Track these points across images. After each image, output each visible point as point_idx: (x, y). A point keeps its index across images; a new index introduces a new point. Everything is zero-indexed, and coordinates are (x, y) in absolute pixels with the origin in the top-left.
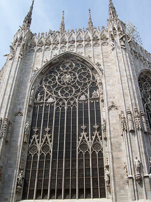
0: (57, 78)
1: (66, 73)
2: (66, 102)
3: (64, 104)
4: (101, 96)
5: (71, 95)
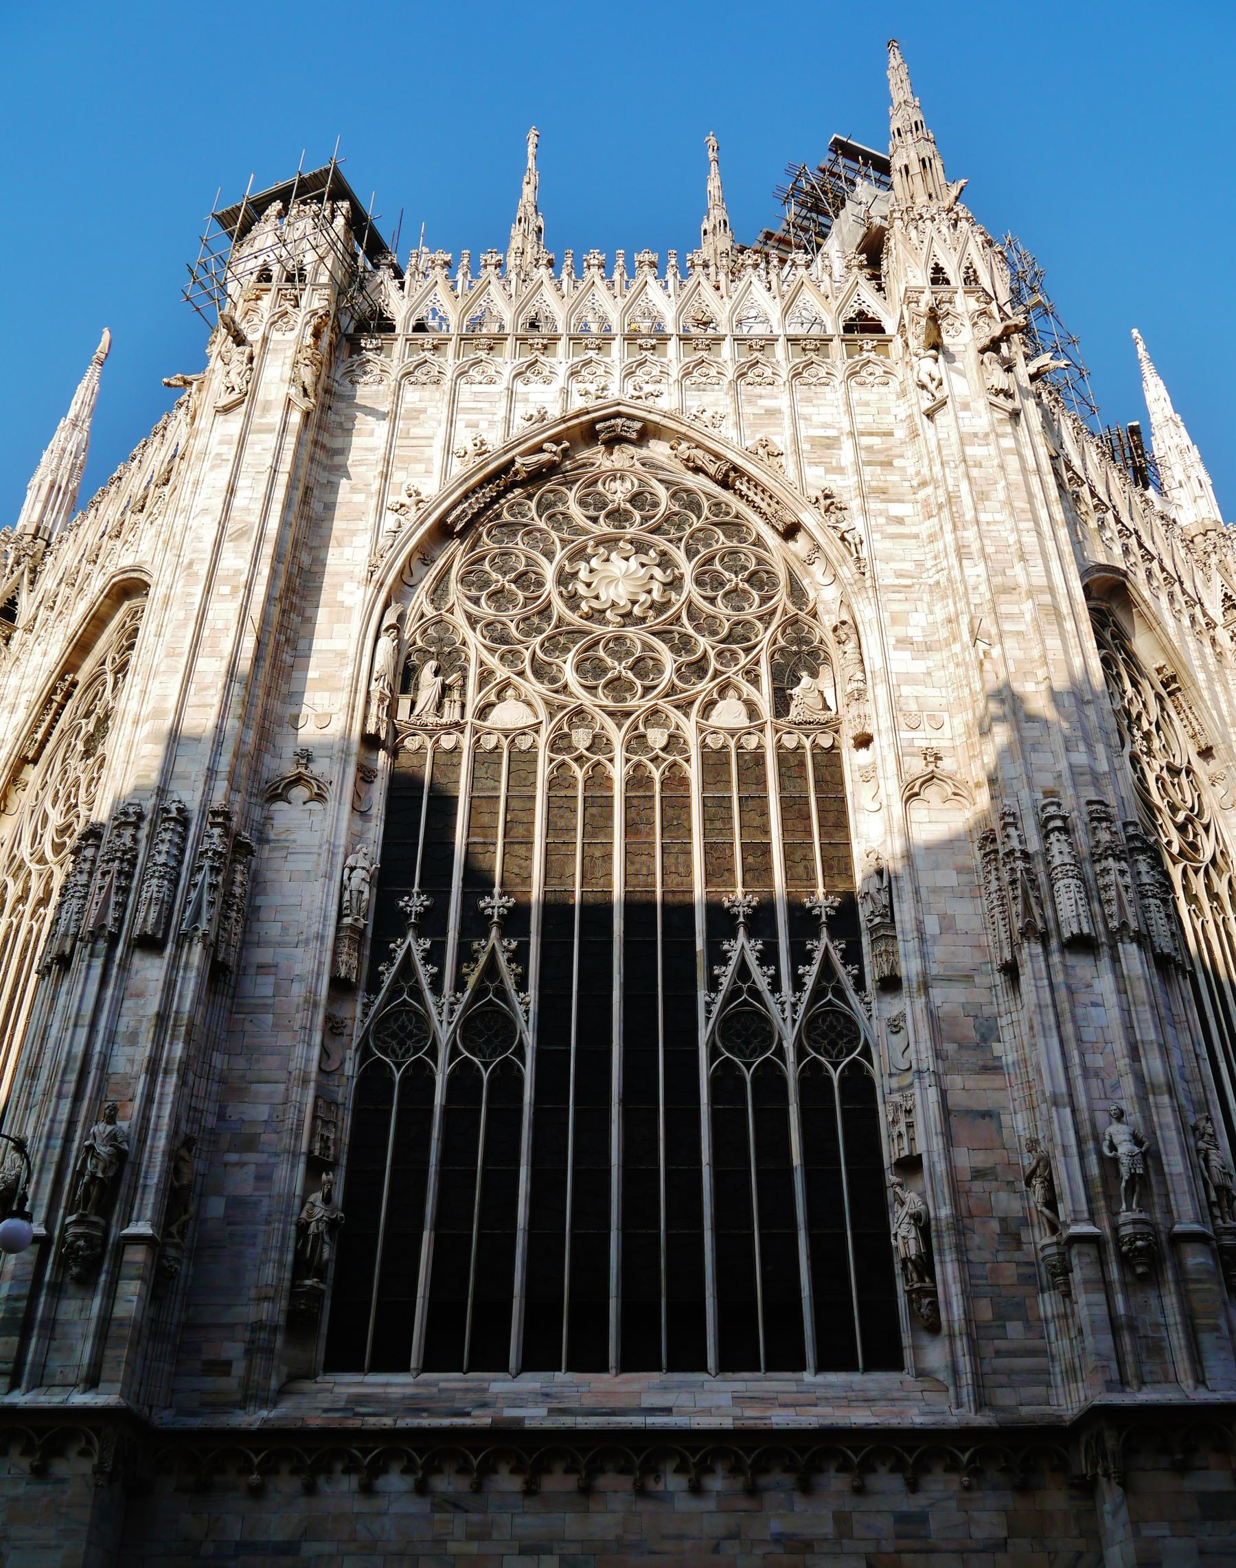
0: (549, 571)
1: (609, 542)
2: (617, 737)
3: (599, 743)
4: (854, 709)
5: (647, 690)
